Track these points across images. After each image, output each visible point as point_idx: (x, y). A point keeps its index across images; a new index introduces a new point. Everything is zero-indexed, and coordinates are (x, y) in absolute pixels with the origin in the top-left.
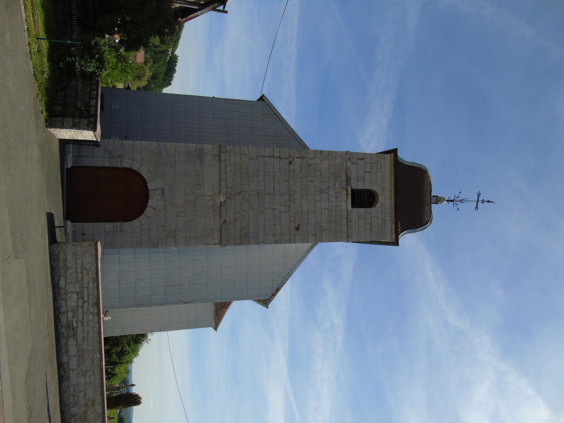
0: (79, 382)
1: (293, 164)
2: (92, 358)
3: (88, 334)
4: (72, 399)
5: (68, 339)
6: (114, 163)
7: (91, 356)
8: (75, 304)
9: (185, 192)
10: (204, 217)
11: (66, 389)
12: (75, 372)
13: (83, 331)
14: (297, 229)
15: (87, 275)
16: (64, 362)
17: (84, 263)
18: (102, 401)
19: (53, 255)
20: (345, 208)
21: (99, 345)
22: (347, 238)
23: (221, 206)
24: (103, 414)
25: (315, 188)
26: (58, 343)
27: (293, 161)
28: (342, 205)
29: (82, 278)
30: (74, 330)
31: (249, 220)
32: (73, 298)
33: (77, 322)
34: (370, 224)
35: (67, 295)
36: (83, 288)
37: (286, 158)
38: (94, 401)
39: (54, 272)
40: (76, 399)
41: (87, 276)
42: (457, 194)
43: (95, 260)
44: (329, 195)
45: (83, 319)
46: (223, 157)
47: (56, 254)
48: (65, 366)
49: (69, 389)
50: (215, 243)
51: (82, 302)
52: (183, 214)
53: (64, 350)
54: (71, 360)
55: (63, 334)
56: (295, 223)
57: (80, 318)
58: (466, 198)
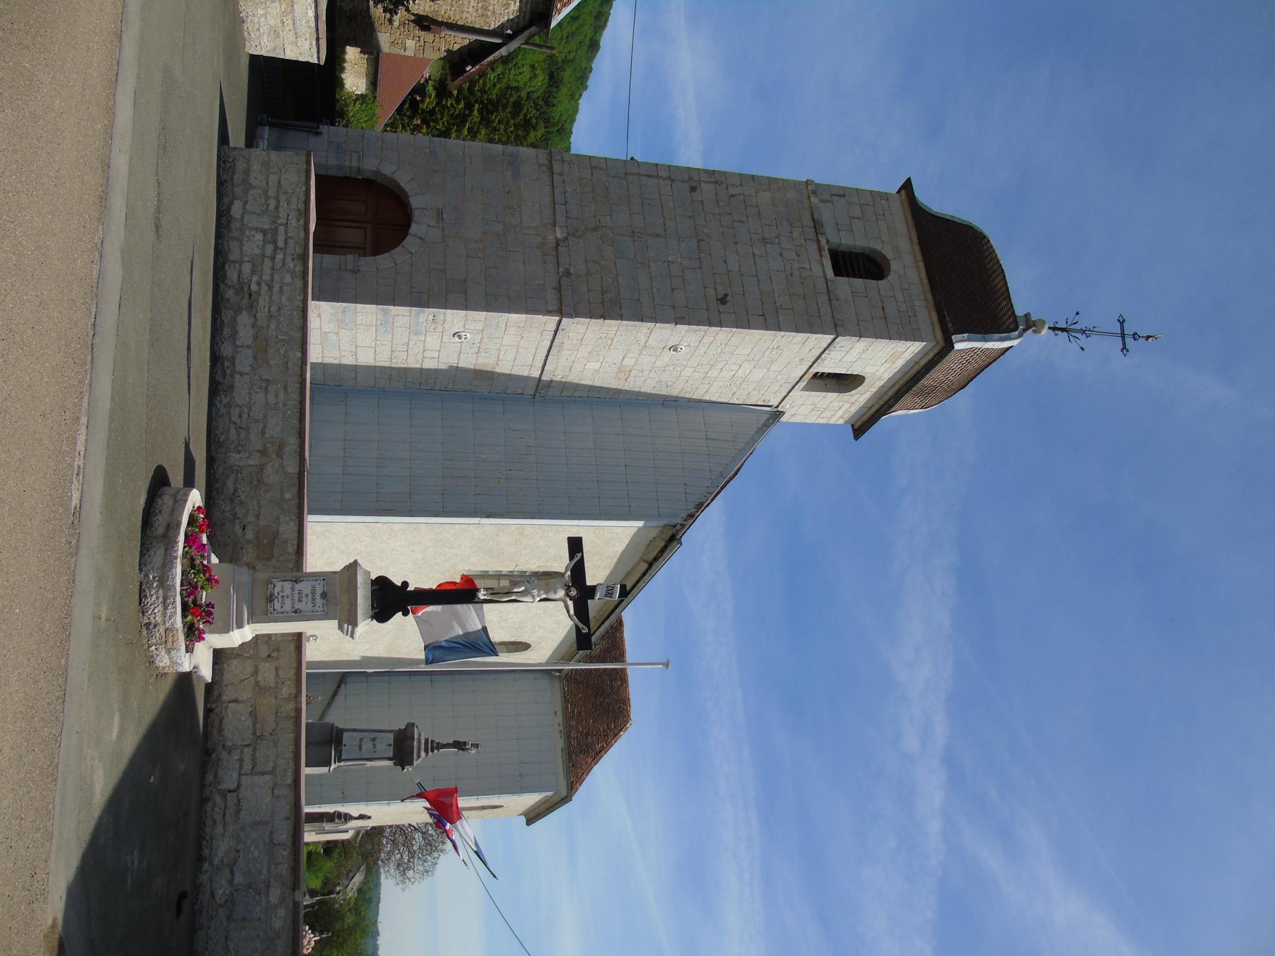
0: (253, 402)
1: (699, 190)
2: (285, 357)
3: (280, 309)
4: (233, 432)
5: (238, 311)
6: (345, 161)
7: (283, 352)
8: (256, 251)
9: (483, 218)
10: (524, 263)
11: (223, 410)
12: (247, 378)
13: (270, 304)
14: (723, 301)
15: (286, 203)
16: (225, 355)
17: (282, 182)
18: (298, 450)
19: (224, 162)
20: (821, 275)
21: (301, 333)
22: (836, 329)
23: (557, 245)
24: (299, 479)
25: (750, 233)
26: (216, 316)
27: (699, 187)
28: (812, 268)
29: (277, 208)
30: (253, 298)
31: (617, 275)
32: (256, 239)
33: (259, 284)
34: (881, 309)
35: (244, 232)
36: (277, 225)
37: (683, 182)
38: (281, 447)
39: (222, 189)
40: (243, 434)
41: (286, 205)
42: (1071, 316)
43: (304, 179)
44: (781, 248)
45: (272, 280)
46: (557, 168)
47: (230, 160)
48: (227, 364)
49: (229, 412)
50: (550, 309)
51: (272, 249)
52: (480, 255)
53: (226, 332)
54: (239, 354)
55: (228, 300)
56: (716, 291)
57: (266, 277)
58: (1094, 327)
